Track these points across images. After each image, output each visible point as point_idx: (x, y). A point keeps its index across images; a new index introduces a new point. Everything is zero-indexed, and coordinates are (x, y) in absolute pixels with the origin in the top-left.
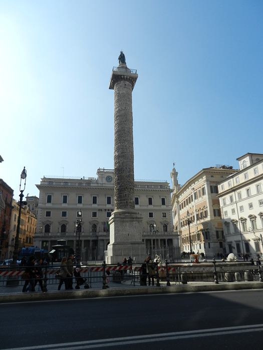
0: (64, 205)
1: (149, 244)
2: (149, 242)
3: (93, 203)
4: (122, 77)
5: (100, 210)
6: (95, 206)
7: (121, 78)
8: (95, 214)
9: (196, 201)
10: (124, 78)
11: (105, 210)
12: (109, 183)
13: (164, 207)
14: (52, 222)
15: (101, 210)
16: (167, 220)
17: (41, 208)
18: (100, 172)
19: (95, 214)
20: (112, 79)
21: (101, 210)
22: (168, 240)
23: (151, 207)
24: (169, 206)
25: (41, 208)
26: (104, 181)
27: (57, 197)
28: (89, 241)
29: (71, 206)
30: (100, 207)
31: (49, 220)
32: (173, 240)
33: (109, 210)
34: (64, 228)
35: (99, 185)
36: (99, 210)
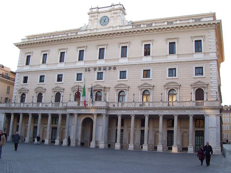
0: (44, 67)
3: (79, 60)
5: (88, 70)
6: (81, 64)
8: (79, 77)
11: (95, 69)
12: (104, 27)
13: (199, 56)
14: (28, 90)
15: (89, 71)
18: (93, 13)
19: (79, 77)
21: (89, 71)
23: (173, 58)
24: (209, 53)
27: (37, 56)
29: (50, 68)
30: (88, 65)
32: (206, 118)
33: (100, 69)
34: (40, 98)
35: (89, 32)
36: (86, 71)
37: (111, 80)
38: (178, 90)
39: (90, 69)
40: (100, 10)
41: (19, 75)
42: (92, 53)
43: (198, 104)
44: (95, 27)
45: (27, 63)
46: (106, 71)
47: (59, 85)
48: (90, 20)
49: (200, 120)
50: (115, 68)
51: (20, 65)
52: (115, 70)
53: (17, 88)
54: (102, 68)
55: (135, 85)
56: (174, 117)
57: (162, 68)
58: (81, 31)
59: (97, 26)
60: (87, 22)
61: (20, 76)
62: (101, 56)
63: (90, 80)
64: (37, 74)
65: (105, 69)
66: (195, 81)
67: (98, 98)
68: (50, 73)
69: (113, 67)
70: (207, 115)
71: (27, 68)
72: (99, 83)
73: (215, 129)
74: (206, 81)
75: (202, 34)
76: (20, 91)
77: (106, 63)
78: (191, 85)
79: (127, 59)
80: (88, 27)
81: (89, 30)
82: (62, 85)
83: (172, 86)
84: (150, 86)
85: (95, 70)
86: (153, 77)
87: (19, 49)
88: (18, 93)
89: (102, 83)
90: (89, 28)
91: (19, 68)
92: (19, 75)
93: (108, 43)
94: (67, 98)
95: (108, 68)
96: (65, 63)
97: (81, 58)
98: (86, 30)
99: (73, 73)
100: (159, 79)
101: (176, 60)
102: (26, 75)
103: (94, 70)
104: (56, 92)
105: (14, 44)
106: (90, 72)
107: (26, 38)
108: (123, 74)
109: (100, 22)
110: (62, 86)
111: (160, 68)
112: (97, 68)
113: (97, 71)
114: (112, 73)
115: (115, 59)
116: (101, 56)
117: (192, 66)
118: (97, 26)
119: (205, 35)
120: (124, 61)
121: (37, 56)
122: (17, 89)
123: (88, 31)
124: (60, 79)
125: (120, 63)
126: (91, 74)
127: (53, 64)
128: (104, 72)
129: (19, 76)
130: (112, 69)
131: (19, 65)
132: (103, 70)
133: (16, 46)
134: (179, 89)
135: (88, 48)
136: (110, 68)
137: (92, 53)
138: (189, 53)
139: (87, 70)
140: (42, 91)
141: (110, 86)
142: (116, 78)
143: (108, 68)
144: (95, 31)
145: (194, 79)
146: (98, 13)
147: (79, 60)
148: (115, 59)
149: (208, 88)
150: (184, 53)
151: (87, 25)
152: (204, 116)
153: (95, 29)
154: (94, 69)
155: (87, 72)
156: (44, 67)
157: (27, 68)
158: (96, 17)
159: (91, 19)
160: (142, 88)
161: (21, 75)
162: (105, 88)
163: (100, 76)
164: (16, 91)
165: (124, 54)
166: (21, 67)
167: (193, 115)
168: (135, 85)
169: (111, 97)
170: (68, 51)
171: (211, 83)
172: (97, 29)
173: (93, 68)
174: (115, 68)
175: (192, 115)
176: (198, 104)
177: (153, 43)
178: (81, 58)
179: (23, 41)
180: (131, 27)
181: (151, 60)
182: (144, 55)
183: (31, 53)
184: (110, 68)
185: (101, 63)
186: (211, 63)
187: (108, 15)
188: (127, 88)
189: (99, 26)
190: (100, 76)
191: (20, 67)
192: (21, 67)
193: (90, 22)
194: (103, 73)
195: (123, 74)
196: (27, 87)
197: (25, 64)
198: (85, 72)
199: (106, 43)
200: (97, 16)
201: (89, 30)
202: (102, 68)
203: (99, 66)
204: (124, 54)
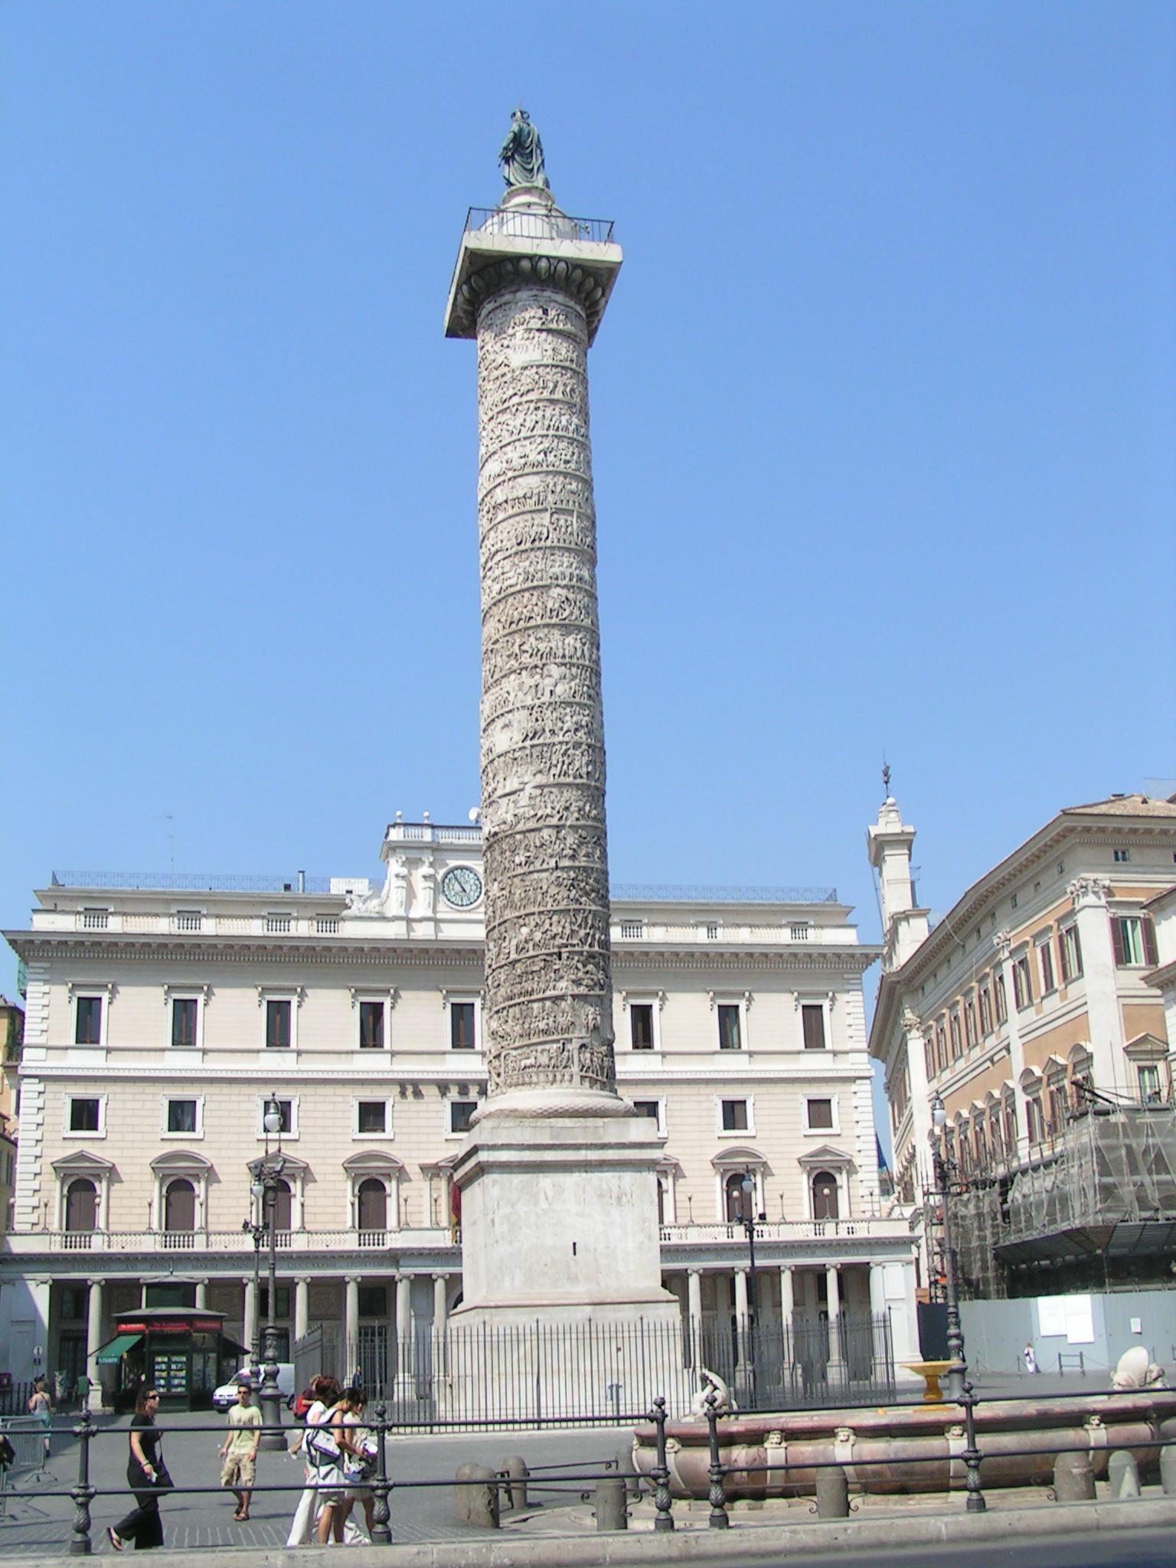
1: (723, 1302)
2: (722, 1284)
4: (525, 264)
5: (411, 1088)
6: (373, 1063)
7: (518, 272)
8: (371, 1115)
9: (1030, 1014)
10: (534, 269)
11: (443, 1087)
15: (418, 1094)
16: (834, 1144)
17: (42, 1078)
19: (371, 1115)
20: (466, 279)
21: (418, 1094)
25: (42, 1078)
28: (340, 1284)
31: (93, 1150)
32: (876, 1275)
33: (463, 1087)
36: (403, 1094)
41: (41, 1087)
76: (62, 1169)
85: (443, 1095)
99: (341, 1099)
113: (454, 1095)
133: (13, 943)
140: (191, 1172)
171: (855, 1154)
182: (636, 1046)
186: (854, 1087)
189: (444, 911)
198: (398, 1098)
200: (431, 865)
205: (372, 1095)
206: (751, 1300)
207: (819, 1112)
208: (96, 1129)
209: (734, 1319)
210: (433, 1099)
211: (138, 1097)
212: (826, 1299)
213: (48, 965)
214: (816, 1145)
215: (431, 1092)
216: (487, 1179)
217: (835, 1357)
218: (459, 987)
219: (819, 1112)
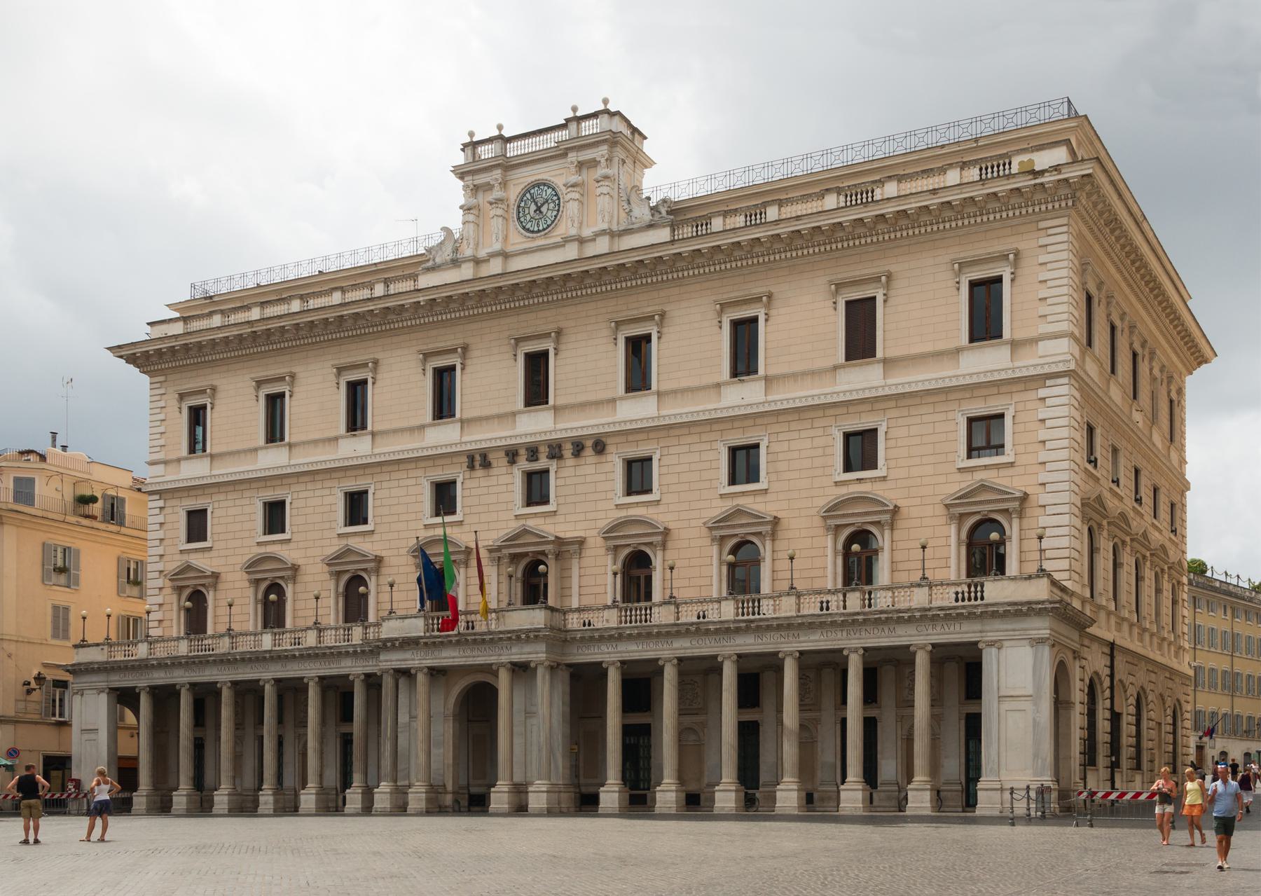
1: (828, 701)
2: (829, 677)
5: (479, 460)
6: (446, 436)
8: (444, 498)
11: (512, 455)
15: (486, 464)
19: (444, 498)
21: (486, 464)
22: (942, 656)
26: (500, 233)
27: (236, 409)
29: (305, 459)
30: (480, 438)
32: (990, 660)
33: (533, 453)
35: (467, 272)
36: (471, 467)
37: (587, 504)
38: (887, 533)
39: (491, 457)
40: (514, 150)
41: (161, 503)
42: (490, 380)
43: (976, 592)
44: (497, 247)
45: (196, 445)
46: (562, 463)
47: (354, 543)
48: (467, 209)
49: (964, 671)
50: (600, 447)
51: (161, 456)
52: (603, 458)
53: (160, 566)
54: (544, 451)
55: (693, 523)
56: (914, 654)
57: (811, 433)
58: (434, 269)
59: (506, 238)
60: (455, 221)
61: (166, 511)
62: (536, 392)
63: (492, 511)
64: (247, 494)
65: (555, 451)
66: (963, 485)
67: (533, 589)
68: (310, 486)
69: (589, 443)
70: (991, 644)
71: (196, 470)
72: (531, 523)
73: (1027, 705)
74: (1014, 482)
75: (997, 247)
77: (559, 426)
78: (947, 506)
79: (654, 399)
80: (465, 242)
81: (466, 260)
82: (368, 539)
83: (857, 518)
84: (758, 518)
86: (773, 477)
87: (146, 378)
88: (168, 591)
89: (548, 520)
90: (468, 252)
91: (160, 469)
92: (161, 503)
93: (562, 325)
94: (397, 604)
95: (568, 450)
96: (373, 434)
97: (443, 407)
98: (455, 263)
100: (802, 487)
101: (876, 388)
102: (195, 503)
103: (506, 459)
104: (346, 577)
105: (116, 350)
106: (494, 471)
107: (177, 315)
108: (638, 476)
109: (519, 218)
110: (367, 547)
111: (804, 434)
112: (522, 452)
113: (524, 464)
114: (590, 469)
115: (597, 404)
116: (536, 392)
117: (950, 416)
118: (506, 238)
119: (1021, 246)
120: (640, 409)
121: (236, 409)
122: (161, 572)
123: (464, 266)
124: (356, 508)
125: (620, 423)
126: (493, 481)
127: (315, 442)
128: (553, 466)
129: (161, 508)
130: (589, 451)
131: (156, 457)
132: (552, 457)
133: (131, 359)
134: (892, 530)
135: (474, 353)
136: (578, 448)
137: (490, 380)
138: (941, 346)
139: (477, 464)
141: (582, 534)
142: (610, 495)
143: (568, 450)
144: (495, 267)
145: (958, 477)
146: (507, 166)
147: (441, 418)
148: (597, 404)
149: (1029, 512)
150: (915, 350)
151: (457, 236)
152: (981, 646)
153: (493, 255)
154: (507, 455)
155: (479, 473)
156: (274, 459)
157: (196, 470)
158: (497, 193)
159: (473, 201)
160: (723, 532)
161: (174, 502)
162: (559, 541)
163: (536, 489)
164: (160, 583)
165: (638, 377)
166: (166, 462)
167: (930, 648)
168: (693, 523)
169: (592, 584)
170: (385, 376)
172: (505, 255)
173: (502, 454)
174: (600, 447)
175: (925, 645)
176: (976, 592)
177: (773, 312)
178: (443, 407)
179: (158, 332)
180: (663, 235)
181: (762, 399)
183: (204, 392)
184: (578, 448)
185: (537, 425)
187: (559, 175)
188: (659, 538)
190: (536, 489)
191: (161, 467)
192: (166, 462)
193: (471, 218)
194: (547, 471)
195: (638, 476)
196: (204, 563)
197: (184, 451)
198: (467, 475)
199: (550, 327)
201: (466, 260)
202: (544, 451)
203: (529, 440)
204: (638, 377)
205: (442, 475)
206: (280, 720)
207: (985, 434)
208: (205, 539)
209: (844, 722)
210: (504, 470)
211: (238, 502)
212: (979, 697)
213: (162, 379)
214: (968, 482)
215: (499, 461)
216: (743, 549)
217: (920, 778)
218: (529, 331)
219: (985, 434)
